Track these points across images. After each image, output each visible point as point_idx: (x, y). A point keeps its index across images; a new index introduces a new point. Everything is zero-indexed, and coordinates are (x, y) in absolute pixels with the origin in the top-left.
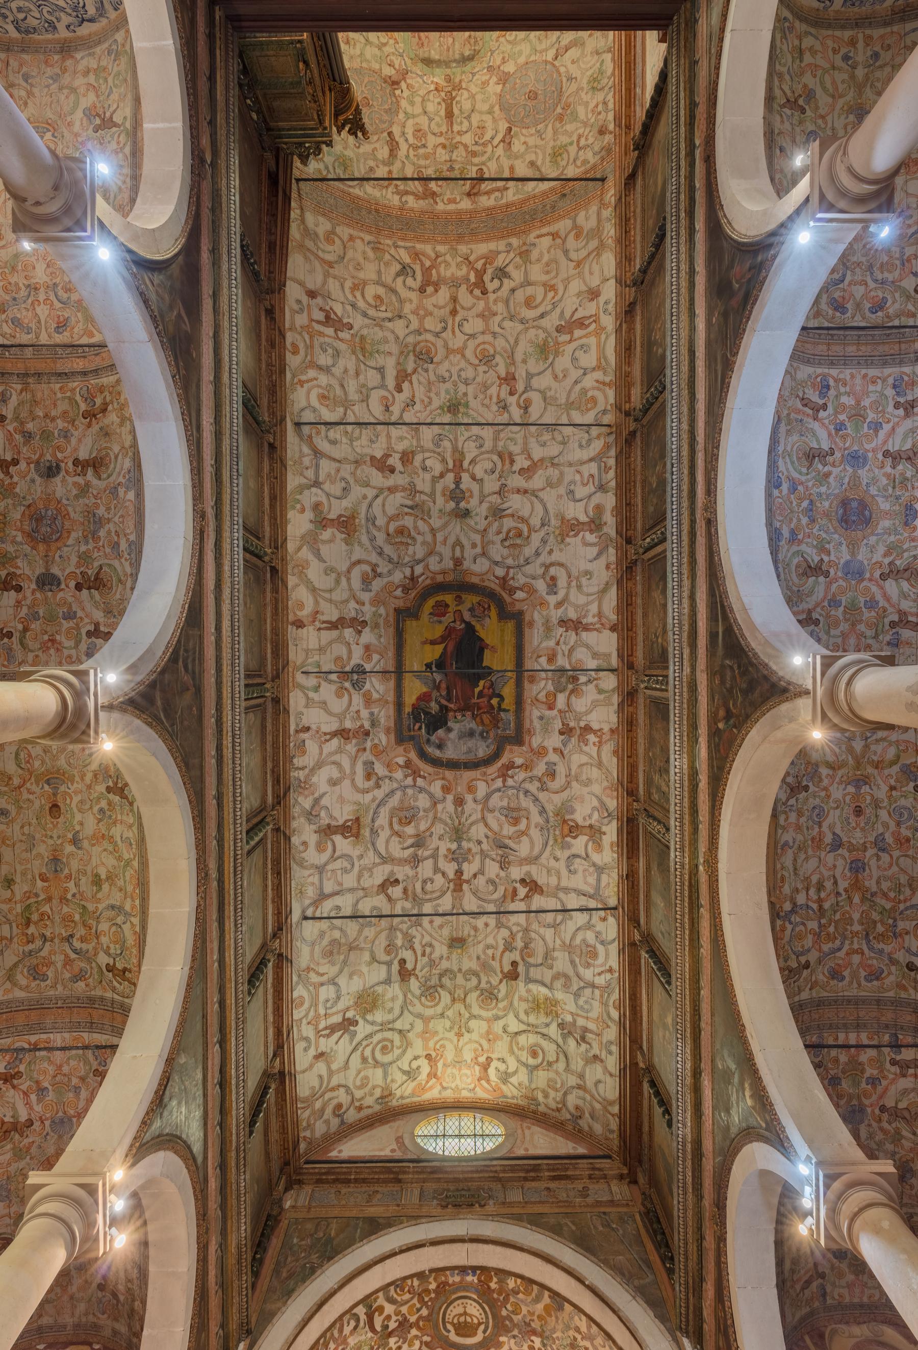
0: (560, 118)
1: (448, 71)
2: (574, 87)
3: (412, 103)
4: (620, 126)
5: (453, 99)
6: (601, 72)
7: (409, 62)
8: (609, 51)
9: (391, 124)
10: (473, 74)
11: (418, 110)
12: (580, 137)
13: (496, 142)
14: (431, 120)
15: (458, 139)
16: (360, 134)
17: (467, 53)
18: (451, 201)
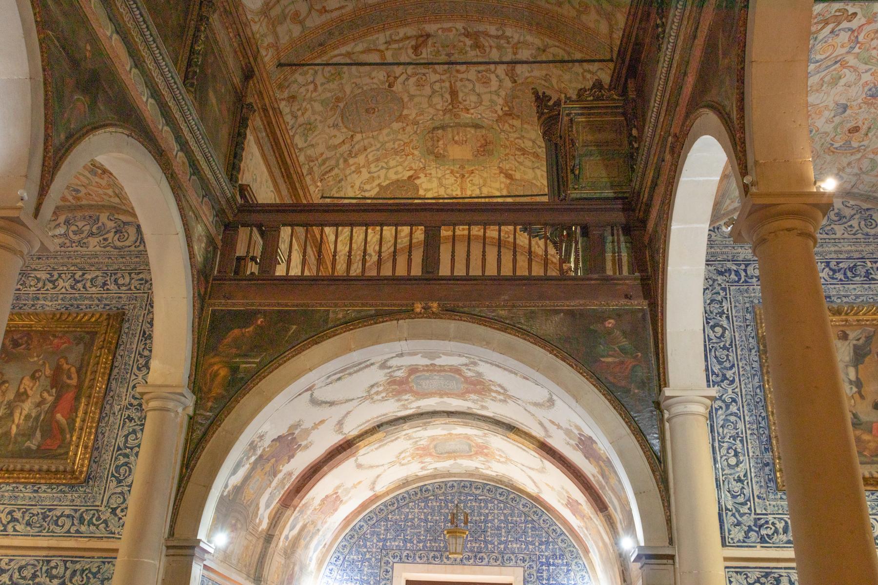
0: (338, 100)
1: (457, 121)
2: (330, 122)
3: (491, 101)
4: (274, 109)
5: (452, 103)
6: (305, 136)
7: (495, 126)
8: (301, 150)
9: (513, 89)
10: (432, 119)
11: (486, 98)
12: (315, 90)
13: (404, 77)
14: (473, 90)
15: (444, 77)
16: (540, 94)
17: (440, 131)
18: (449, 30)
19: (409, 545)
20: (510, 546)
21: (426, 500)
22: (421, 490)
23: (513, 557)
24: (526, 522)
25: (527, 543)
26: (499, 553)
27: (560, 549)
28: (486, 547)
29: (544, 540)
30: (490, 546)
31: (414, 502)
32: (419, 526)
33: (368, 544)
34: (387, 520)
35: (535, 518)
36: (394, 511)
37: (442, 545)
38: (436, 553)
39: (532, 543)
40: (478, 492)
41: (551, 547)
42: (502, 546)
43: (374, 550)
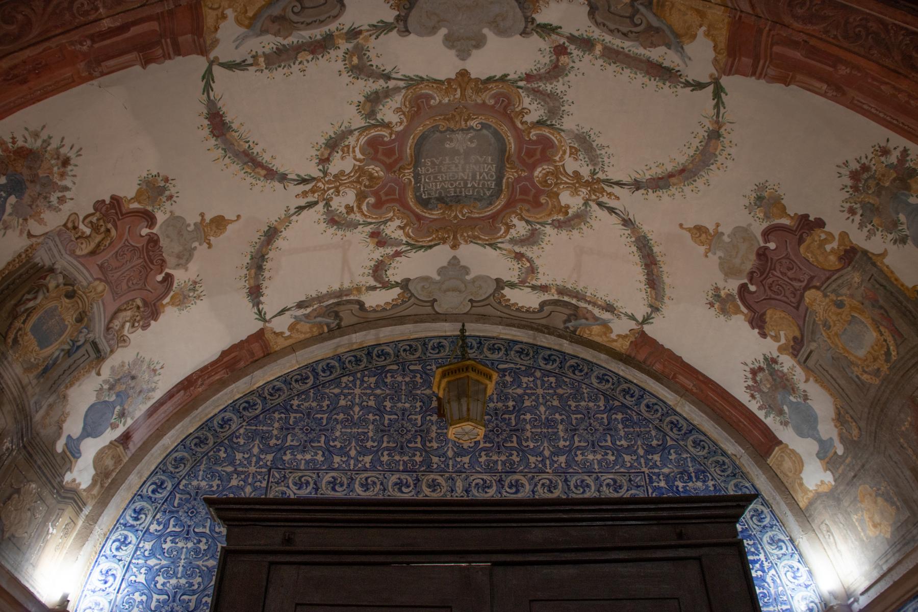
19: (337, 459)
20: (579, 458)
21: (381, 372)
22: (369, 354)
23: (589, 481)
24: (610, 410)
25: (618, 452)
26: (555, 472)
27: (693, 459)
28: (524, 459)
29: (654, 443)
30: (532, 459)
31: (353, 374)
32: (363, 421)
33: (239, 456)
34: (287, 408)
35: (629, 401)
36: (306, 392)
37: (418, 459)
38: (404, 476)
39: (630, 450)
40: (495, 356)
41: (673, 456)
42: (562, 459)
43: (252, 469)
